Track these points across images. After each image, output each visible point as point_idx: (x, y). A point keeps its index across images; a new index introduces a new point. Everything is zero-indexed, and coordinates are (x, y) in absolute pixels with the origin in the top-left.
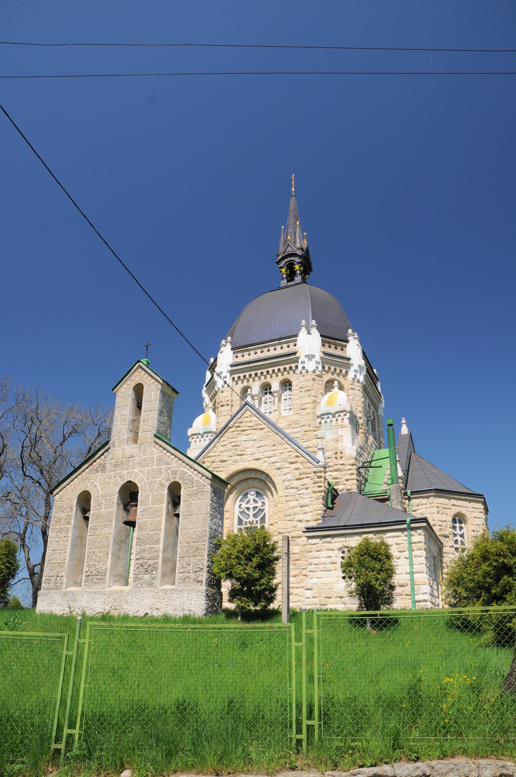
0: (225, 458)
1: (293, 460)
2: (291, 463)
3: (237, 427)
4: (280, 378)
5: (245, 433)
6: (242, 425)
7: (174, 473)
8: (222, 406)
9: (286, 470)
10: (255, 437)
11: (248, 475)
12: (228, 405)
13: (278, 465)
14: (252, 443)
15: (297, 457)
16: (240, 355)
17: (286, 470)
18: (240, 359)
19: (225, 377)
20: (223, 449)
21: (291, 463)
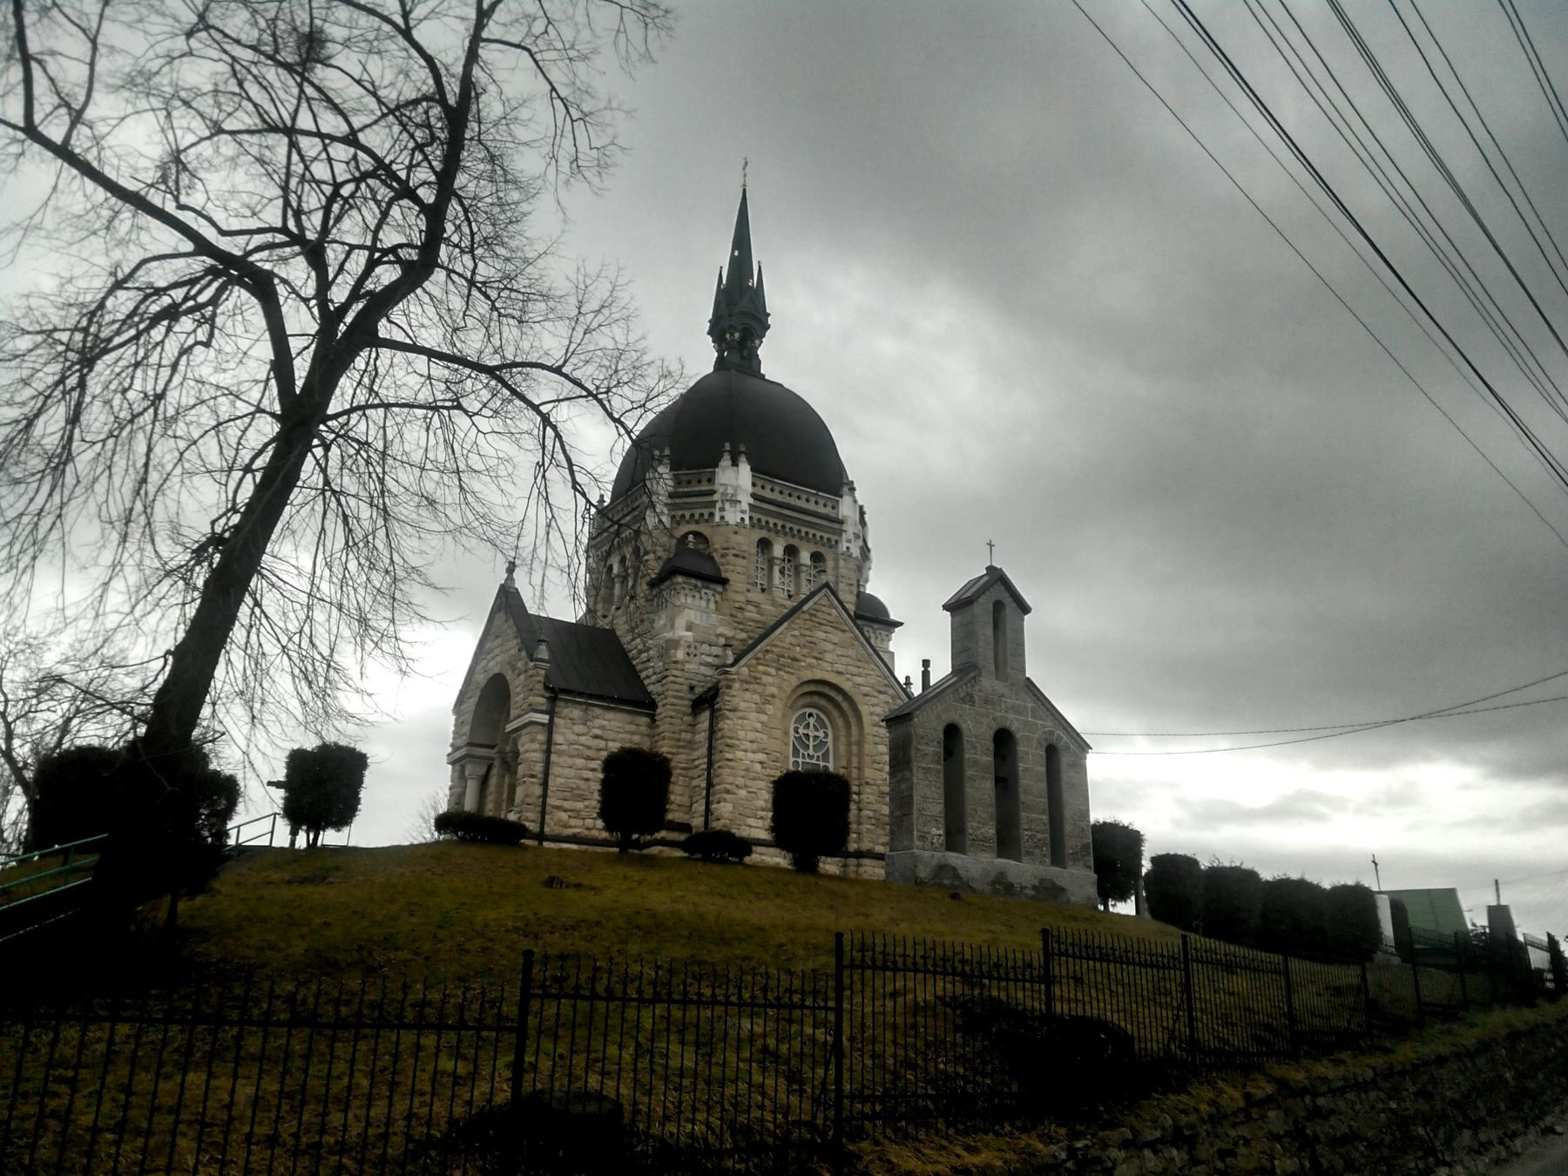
0: (798, 656)
1: (882, 689)
2: (880, 692)
3: (811, 615)
4: (814, 548)
5: (823, 628)
6: (819, 614)
7: (1052, 733)
8: (736, 556)
9: (874, 700)
10: (836, 640)
11: (820, 688)
12: (744, 558)
13: (866, 690)
14: (831, 647)
15: (886, 686)
16: (760, 483)
17: (874, 700)
18: (759, 491)
19: (743, 512)
20: (793, 641)
21: (880, 692)
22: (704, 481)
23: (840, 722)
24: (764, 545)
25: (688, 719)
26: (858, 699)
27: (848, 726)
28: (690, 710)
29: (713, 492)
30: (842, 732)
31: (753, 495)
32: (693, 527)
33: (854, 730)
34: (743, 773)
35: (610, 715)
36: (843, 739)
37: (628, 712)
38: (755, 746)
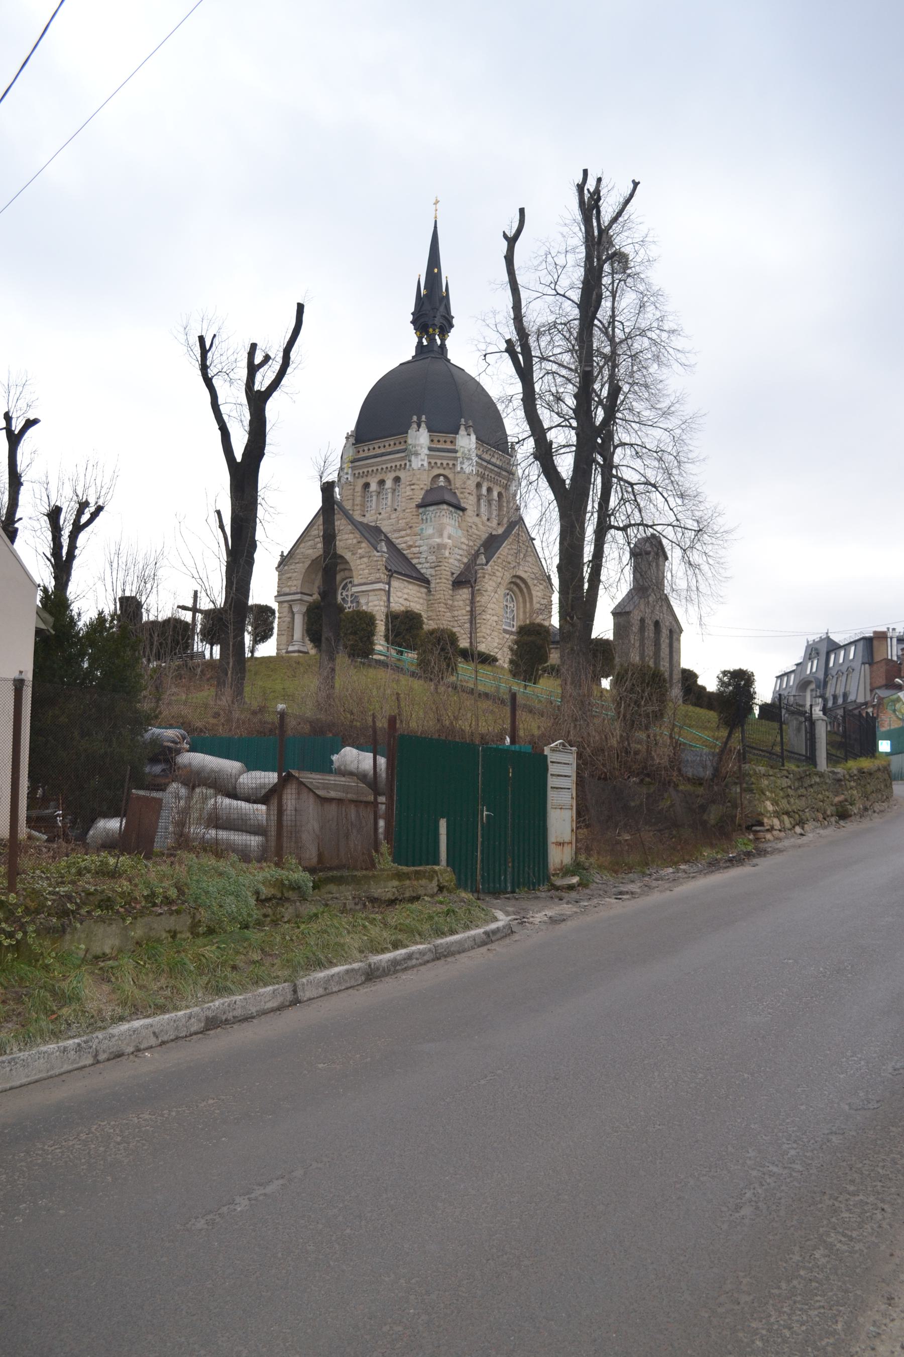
22: (449, 443)
23: (521, 599)
24: (479, 485)
25: (450, 592)
26: (532, 587)
27: (525, 602)
28: (451, 587)
29: (456, 451)
30: (521, 605)
31: (430, 449)
32: (441, 471)
33: (528, 605)
34: (489, 627)
35: (411, 587)
36: (521, 610)
37: (418, 585)
38: (493, 612)
